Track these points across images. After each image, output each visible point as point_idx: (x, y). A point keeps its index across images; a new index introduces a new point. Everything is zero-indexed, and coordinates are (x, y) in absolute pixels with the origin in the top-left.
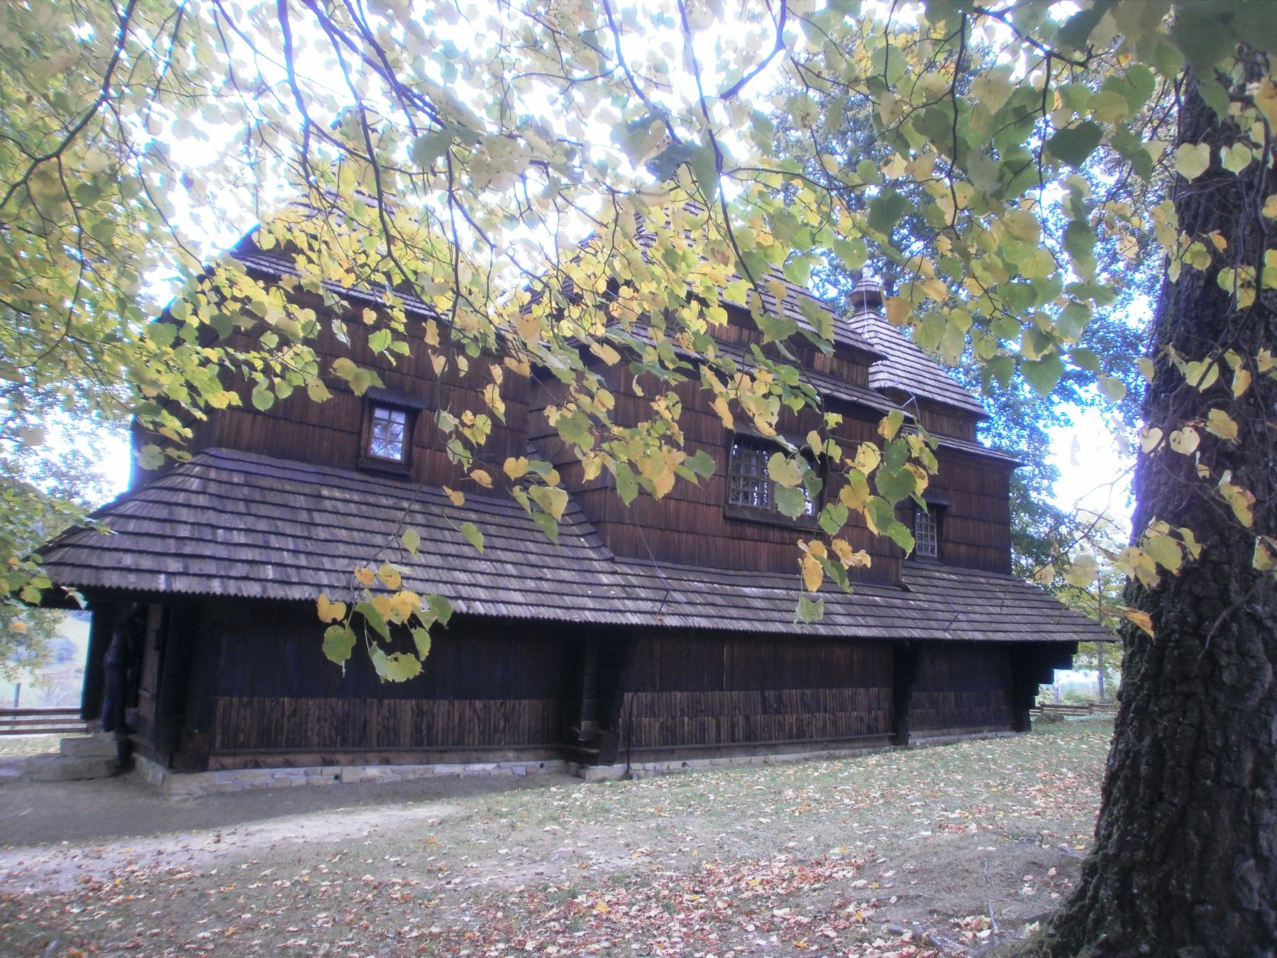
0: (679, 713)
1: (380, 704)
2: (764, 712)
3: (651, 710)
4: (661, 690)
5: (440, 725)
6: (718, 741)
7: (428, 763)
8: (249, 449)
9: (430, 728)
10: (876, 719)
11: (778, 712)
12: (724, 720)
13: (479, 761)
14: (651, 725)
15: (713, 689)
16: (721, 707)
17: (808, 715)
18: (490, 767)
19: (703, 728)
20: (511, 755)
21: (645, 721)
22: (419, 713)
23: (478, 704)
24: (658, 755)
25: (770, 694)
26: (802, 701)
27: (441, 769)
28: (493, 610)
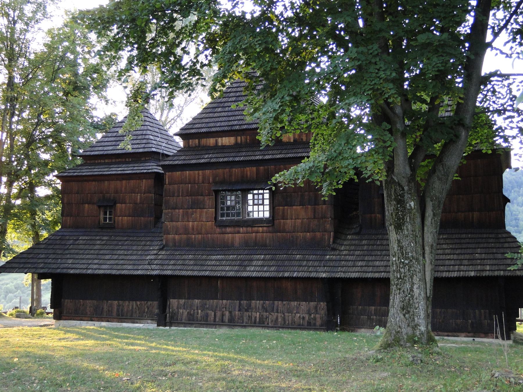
0: (196, 308)
1: (107, 302)
2: (239, 311)
3: (184, 307)
4: (189, 298)
5: (125, 310)
6: (215, 321)
7: (121, 322)
8: (69, 227)
9: (122, 311)
10: (315, 319)
11: (247, 310)
12: (219, 314)
13: (137, 323)
14: (184, 313)
15: (213, 299)
16: (217, 307)
17: (265, 314)
18: (141, 325)
19: (207, 315)
20: (149, 321)
22: (119, 306)
23: (138, 303)
24: (185, 325)
25: (244, 302)
26: (263, 307)
27: (125, 325)
28: (118, 273)
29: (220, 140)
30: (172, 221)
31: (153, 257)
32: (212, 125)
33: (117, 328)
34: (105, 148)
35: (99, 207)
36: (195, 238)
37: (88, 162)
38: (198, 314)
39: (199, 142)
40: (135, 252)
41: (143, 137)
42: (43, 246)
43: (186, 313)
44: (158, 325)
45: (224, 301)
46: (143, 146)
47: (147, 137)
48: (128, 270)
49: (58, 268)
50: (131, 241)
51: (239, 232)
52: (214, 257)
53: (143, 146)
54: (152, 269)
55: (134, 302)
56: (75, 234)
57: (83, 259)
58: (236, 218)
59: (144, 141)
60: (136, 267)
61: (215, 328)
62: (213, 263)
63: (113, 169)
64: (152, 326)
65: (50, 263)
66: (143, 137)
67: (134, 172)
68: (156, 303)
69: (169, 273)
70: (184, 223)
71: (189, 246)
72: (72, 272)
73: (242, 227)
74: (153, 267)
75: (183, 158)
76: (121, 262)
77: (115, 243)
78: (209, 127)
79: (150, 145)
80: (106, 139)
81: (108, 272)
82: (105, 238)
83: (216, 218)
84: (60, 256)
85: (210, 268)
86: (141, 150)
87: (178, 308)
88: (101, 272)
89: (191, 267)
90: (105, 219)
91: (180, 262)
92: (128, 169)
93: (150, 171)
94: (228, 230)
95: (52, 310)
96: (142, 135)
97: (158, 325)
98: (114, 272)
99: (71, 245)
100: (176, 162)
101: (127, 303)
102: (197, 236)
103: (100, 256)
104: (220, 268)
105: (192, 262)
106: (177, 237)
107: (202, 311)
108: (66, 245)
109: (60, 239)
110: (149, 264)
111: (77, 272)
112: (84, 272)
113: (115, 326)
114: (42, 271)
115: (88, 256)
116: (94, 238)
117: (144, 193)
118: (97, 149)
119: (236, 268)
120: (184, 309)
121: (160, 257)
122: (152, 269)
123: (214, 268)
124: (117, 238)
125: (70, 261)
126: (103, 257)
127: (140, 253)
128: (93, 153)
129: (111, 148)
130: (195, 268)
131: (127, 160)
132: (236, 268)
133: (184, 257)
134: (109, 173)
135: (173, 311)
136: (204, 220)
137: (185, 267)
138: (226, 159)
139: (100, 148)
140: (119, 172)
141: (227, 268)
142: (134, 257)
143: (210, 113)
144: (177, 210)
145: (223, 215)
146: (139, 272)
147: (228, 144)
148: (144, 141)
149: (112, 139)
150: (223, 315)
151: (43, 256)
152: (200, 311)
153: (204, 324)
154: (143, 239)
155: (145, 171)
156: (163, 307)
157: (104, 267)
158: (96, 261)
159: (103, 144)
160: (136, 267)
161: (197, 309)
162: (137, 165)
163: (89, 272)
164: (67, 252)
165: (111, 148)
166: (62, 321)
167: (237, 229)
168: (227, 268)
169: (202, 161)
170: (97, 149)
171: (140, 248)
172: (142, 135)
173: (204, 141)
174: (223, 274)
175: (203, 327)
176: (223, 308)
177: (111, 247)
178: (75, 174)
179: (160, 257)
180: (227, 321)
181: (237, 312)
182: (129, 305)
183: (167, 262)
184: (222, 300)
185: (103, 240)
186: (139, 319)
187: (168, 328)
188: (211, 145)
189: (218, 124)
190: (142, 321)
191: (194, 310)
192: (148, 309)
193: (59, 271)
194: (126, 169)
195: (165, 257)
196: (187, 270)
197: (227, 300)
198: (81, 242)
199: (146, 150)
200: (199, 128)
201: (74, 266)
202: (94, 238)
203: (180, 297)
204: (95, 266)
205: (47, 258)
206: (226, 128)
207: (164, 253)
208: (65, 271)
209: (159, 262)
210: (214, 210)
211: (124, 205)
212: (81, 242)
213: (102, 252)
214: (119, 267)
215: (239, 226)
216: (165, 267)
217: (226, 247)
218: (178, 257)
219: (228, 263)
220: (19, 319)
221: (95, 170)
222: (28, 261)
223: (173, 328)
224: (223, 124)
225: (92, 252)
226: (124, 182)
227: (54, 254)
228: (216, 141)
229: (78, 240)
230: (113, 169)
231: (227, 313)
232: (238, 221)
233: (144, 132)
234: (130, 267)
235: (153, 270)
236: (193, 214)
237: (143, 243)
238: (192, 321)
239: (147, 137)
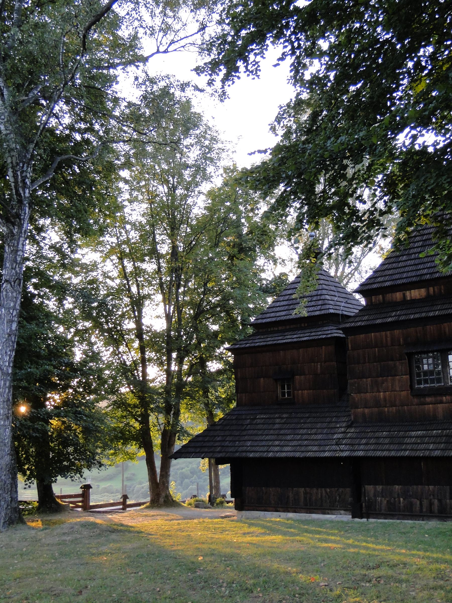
6: (421, 511)
12: (425, 502)
13: (328, 514)
14: (382, 502)
18: (333, 517)
19: (411, 504)
20: (342, 512)
21: (379, 499)
22: (305, 493)
23: (328, 490)
24: (386, 516)
28: (302, 455)
29: (408, 293)
30: (359, 392)
31: (340, 436)
32: (397, 276)
33: (306, 520)
34: (278, 314)
35: (276, 380)
36: (388, 411)
37: (261, 330)
38: (400, 503)
39: (383, 298)
40: (320, 431)
41: (319, 298)
42: (218, 428)
43: (385, 502)
44: (353, 517)
45: (431, 487)
46: (319, 308)
47: (323, 297)
48: (313, 452)
49: (237, 452)
50: (314, 417)
51: (441, 402)
52: (413, 433)
53: (319, 308)
54: (340, 450)
55: (323, 489)
56: (251, 412)
57: (262, 440)
58: (436, 385)
59: (320, 302)
60: (322, 448)
61: (423, 520)
62: (413, 440)
63: (288, 337)
64: (346, 517)
65: (227, 446)
66: (319, 298)
67: (311, 338)
68: (348, 490)
69: (361, 454)
70: (374, 394)
71: (382, 421)
72: (251, 455)
73: (445, 395)
74: (342, 447)
75: (366, 318)
76: (305, 443)
77: (296, 420)
78: (393, 280)
79: (327, 307)
80: (278, 304)
81: (291, 455)
82: (285, 416)
83: (411, 387)
84: (237, 438)
85: (409, 447)
86: (317, 313)
87: (375, 496)
88: (283, 455)
89: (387, 447)
90: (283, 394)
91: (372, 441)
92: (305, 336)
93: (329, 336)
94: (428, 399)
95: (233, 499)
96: (317, 295)
97: (353, 517)
98: (297, 455)
99: (247, 425)
100: (359, 324)
101: (315, 490)
102: (391, 409)
103: (280, 437)
104: (423, 446)
105: (387, 441)
106: (366, 411)
107: (404, 499)
108: (243, 425)
109: (236, 419)
110: (337, 444)
111: (257, 455)
112: (265, 455)
113: (304, 518)
114: (219, 455)
115: (267, 438)
116: (272, 416)
117: (325, 362)
118: (268, 315)
119: (442, 446)
120: (383, 497)
121: (349, 435)
122: (340, 450)
123: (415, 447)
124: (299, 415)
125: (249, 443)
126: (284, 438)
127: (325, 431)
128: (264, 321)
129: (283, 313)
130: (392, 447)
131: (303, 325)
132: (442, 446)
133: (377, 434)
134: (284, 341)
135: (369, 500)
136: (398, 389)
137: (380, 447)
138: (417, 316)
139: (272, 315)
140: (295, 340)
141: (431, 446)
142: (319, 437)
143: (393, 263)
144: (365, 380)
145: (419, 383)
146: (327, 454)
147: (418, 297)
148: (320, 302)
149: (285, 303)
150: (431, 504)
151: (219, 439)
152: (402, 499)
153: (409, 515)
154: (327, 414)
155: (324, 336)
156: (358, 494)
157: (286, 449)
158: (277, 443)
159: (274, 309)
160: (322, 448)
161: (399, 497)
162: (314, 330)
163: (271, 455)
164: (245, 433)
165: (283, 313)
166: (244, 512)
167: (439, 398)
168: (431, 446)
169: (390, 320)
170: (268, 315)
171: (325, 425)
172: (317, 295)
173: (389, 297)
174: (427, 453)
175: (408, 519)
176: (430, 495)
177: (292, 426)
178: (248, 345)
179: (349, 435)
180: (436, 511)
181: (448, 501)
182: (318, 493)
183: (357, 441)
184: (428, 485)
185: (283, 418)
186: (331, 510)
187: (364, 520)
188: (398, 300)
189: (405, 275)
190: (334, 512)
191: (395, 499)
192: (340, 497)
193: (237, 455)
194: (302, 335)
195: (354, 435)
196: (382, 450)
197: (435, 485)
198: (259, 421)
199: (323, 312)
200: (382, 282)
201: (254, 449)
202: (272, 416)
203: (376, 483)
204: (277, 449)
205: (224, 441)
206: (414, 279)
207: (353, 430)
208: (244, 454)
209: (349, 441)
210: (408, 376)
211: (303, 377)
212: (259, 421)
213: (282, 432)
214: (303, 449)
215: (442, 395)
216: (356, 447)
217: (426, 421)
218: (370, 435)
219: (432, 440)
220: (198, 509)
221: (269, 339)
222: (204, 445)
223: (371, 520)
224: (410, 274)
225: (272, 432)
226: (301, 350)
227: (231, 435)
228: (404, 295)
229: (255, 419)
230: (288, 337)
231: (436, 502)
232: (439, 388)
233: (320, 292)
234: (315, 448)
235: (342, 451)
236: (383, 383)
237: (328, 420)
238: (393, 512)
239: (323, 297)
